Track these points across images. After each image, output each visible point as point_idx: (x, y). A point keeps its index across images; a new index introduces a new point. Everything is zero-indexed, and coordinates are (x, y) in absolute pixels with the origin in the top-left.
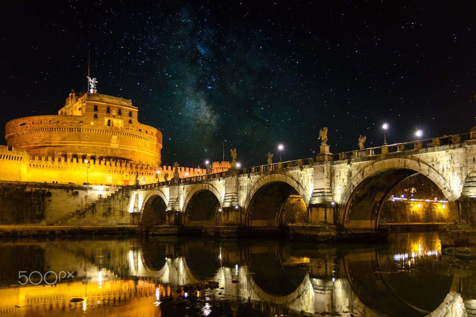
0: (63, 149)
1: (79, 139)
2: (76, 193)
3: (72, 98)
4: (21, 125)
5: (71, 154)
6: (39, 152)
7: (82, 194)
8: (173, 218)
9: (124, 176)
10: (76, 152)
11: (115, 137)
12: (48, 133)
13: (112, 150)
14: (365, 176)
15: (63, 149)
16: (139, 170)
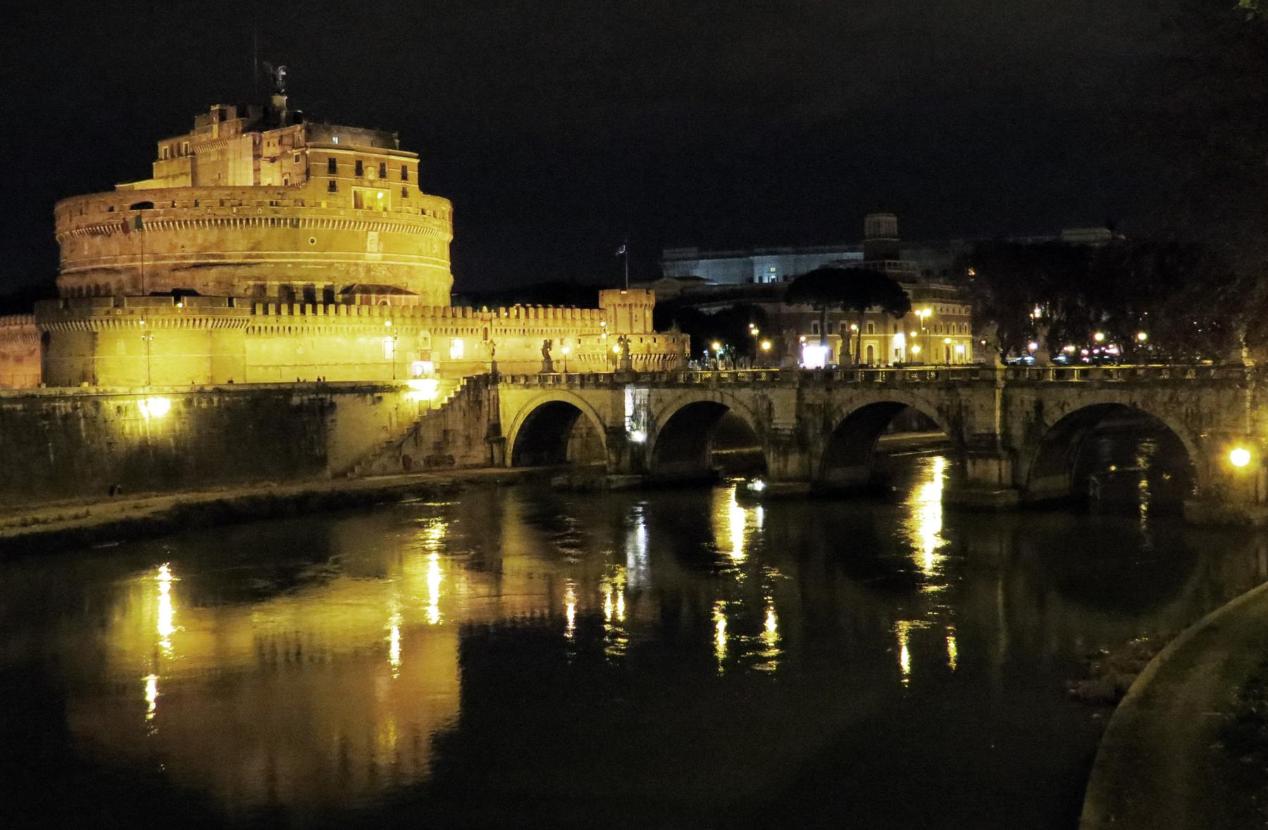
0: (255, 271)
1: (296, 246)
2: (380, 398)
3: (223, 117)
4: (133, 207)
5: (276, 283)
6: (193, 278)
7: (389, 400)
8: (628, 458)
9: (421, 341)
10: (290, 278)
11: (373, 236)
12: (216, 231)
13: (368, 269)
14: (1067, 411)
15: (255, 271)
16: (449, 321)
